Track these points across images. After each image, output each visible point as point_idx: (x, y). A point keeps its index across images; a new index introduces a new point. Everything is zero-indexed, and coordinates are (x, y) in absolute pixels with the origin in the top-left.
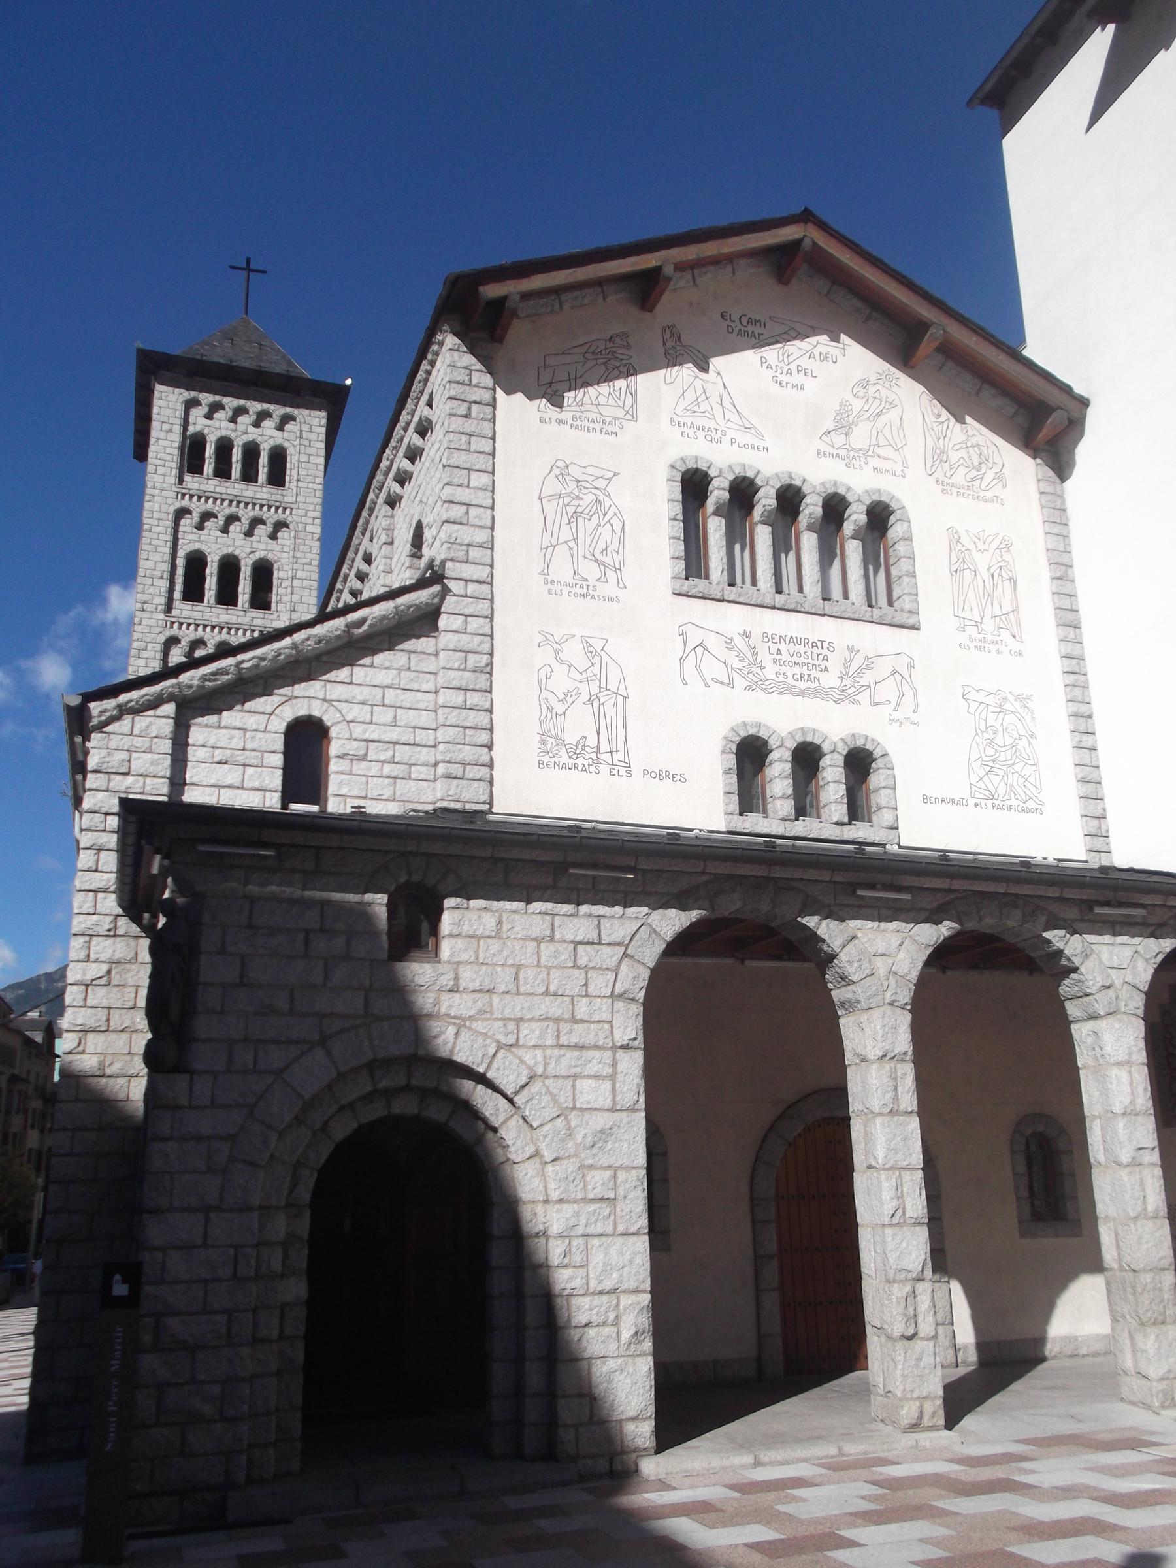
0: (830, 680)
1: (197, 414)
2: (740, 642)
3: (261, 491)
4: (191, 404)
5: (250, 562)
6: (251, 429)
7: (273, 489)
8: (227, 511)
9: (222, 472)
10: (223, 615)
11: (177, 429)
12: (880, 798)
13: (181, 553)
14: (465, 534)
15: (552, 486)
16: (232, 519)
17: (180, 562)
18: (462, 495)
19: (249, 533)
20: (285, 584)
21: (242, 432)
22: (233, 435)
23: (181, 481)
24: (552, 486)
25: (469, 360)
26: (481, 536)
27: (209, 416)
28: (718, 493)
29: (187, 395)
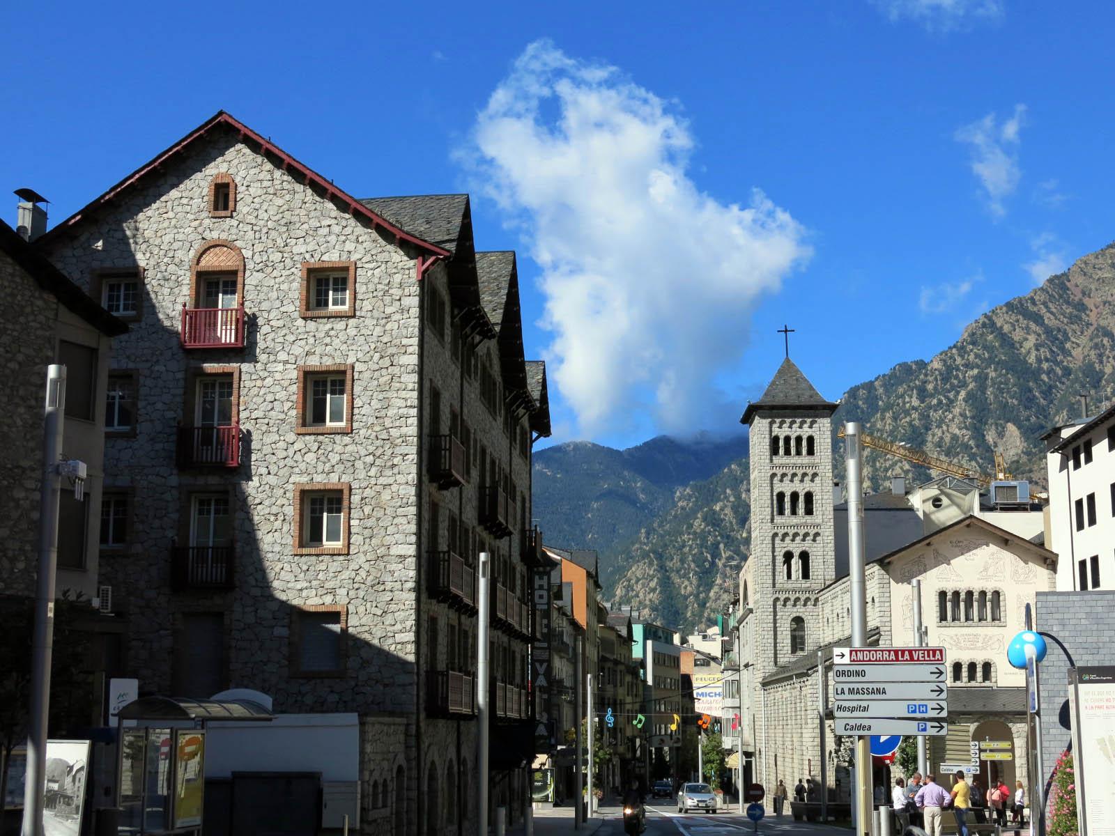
0: (979, 644)
1: (775, 426)
2: (955, 638)
3: (805, 459)
4: (771, 424)
5: (803, 494)
6: (798, 429)
7: (810, 457)
8: (792, 472)
9: (787, 452)
10: (794, 520)
11: (767, 436)
12: (993, 674)
13: (775, 494)
14: (884, 619)
15: (905, 602)
16: (794, 475)
17: (775, 498)
18: (883, 609)
19: (802, 481)
20: (819, 502)
21: (794, 432)
22: (790, 434)
23: (771, 460)
24: (905, 602)
25: (883, 572)
26: (888, 619)
27: (780, 427)
28: (949, 596)
29: (770, 420)
